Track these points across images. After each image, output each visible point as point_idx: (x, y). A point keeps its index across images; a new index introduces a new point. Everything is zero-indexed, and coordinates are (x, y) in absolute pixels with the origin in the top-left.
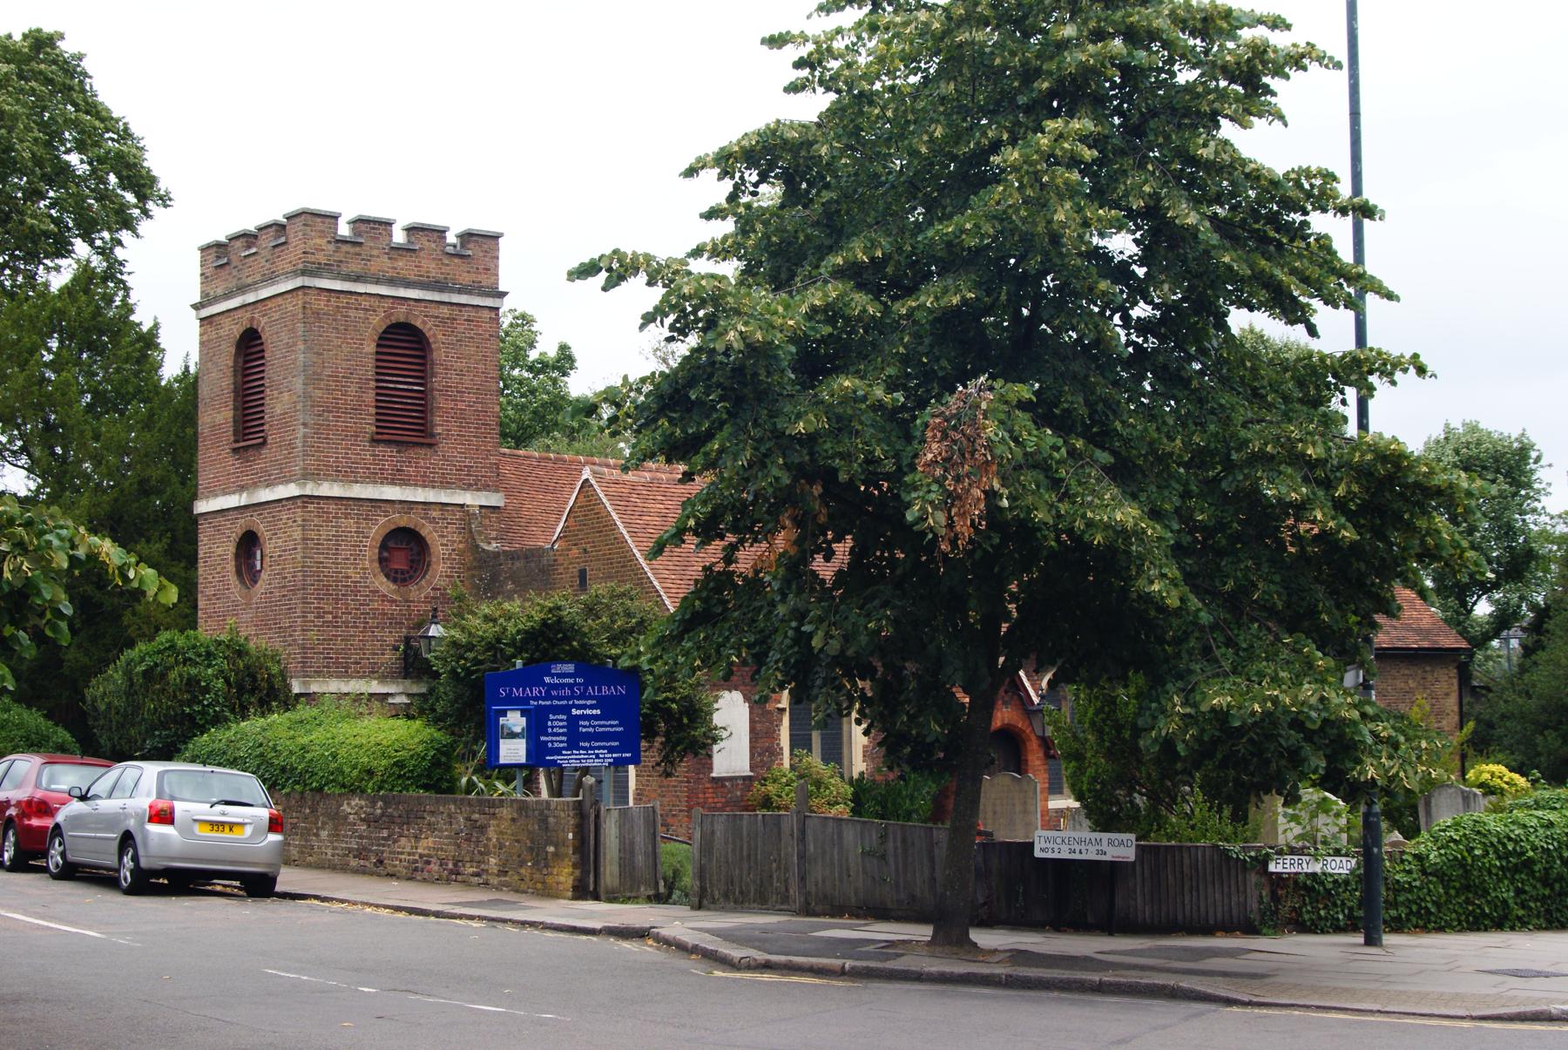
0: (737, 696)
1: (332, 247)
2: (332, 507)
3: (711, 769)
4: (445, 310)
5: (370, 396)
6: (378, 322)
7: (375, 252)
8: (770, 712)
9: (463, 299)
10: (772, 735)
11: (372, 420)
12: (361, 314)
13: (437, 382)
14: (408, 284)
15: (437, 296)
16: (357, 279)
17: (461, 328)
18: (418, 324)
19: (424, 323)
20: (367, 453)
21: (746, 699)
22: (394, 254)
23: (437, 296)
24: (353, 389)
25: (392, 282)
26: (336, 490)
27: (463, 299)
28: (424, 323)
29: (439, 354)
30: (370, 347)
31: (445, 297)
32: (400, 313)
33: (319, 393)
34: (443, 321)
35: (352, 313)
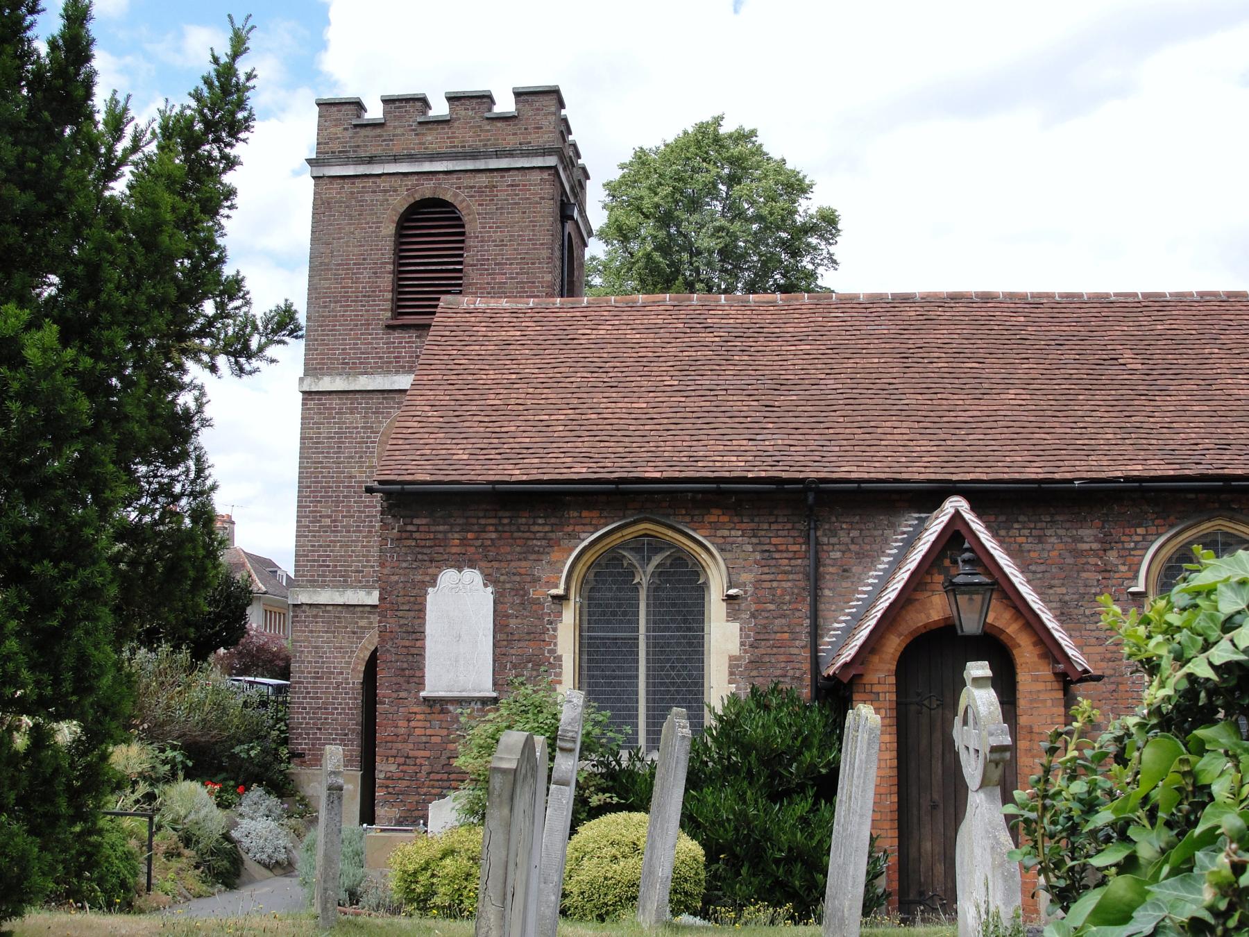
0: (472, 577)
1: (350, 133)
2: (335, 402)
3: (421, 684)
4: (483, 179)
5: (386, 281)
6: (400, 202)
7: (399, 131)
8: (536, 602)
9: (504, 163)
10: (541, 635)
11: (388, 305)
12: (380, 197)
13: (468, 257)
14: (433, 157)
15: (470, 165)
16: (371, 160)
17: (502, 195)
18: (448, 197)
19: (456, 195)
20: (380, 341)
21: (489, 579)
22: (422, 130)
23: (470, 165)
24: (365, 275)
25: (411, 158)
26: (339, 384)
27: (504, 163)
28: (456, 195)
29: (473, 226)
30: (389, 229)
31: (480, 164)
32: (427, 190)
33: (326, 284)
34: (480, 191)
35: (368, 197)
